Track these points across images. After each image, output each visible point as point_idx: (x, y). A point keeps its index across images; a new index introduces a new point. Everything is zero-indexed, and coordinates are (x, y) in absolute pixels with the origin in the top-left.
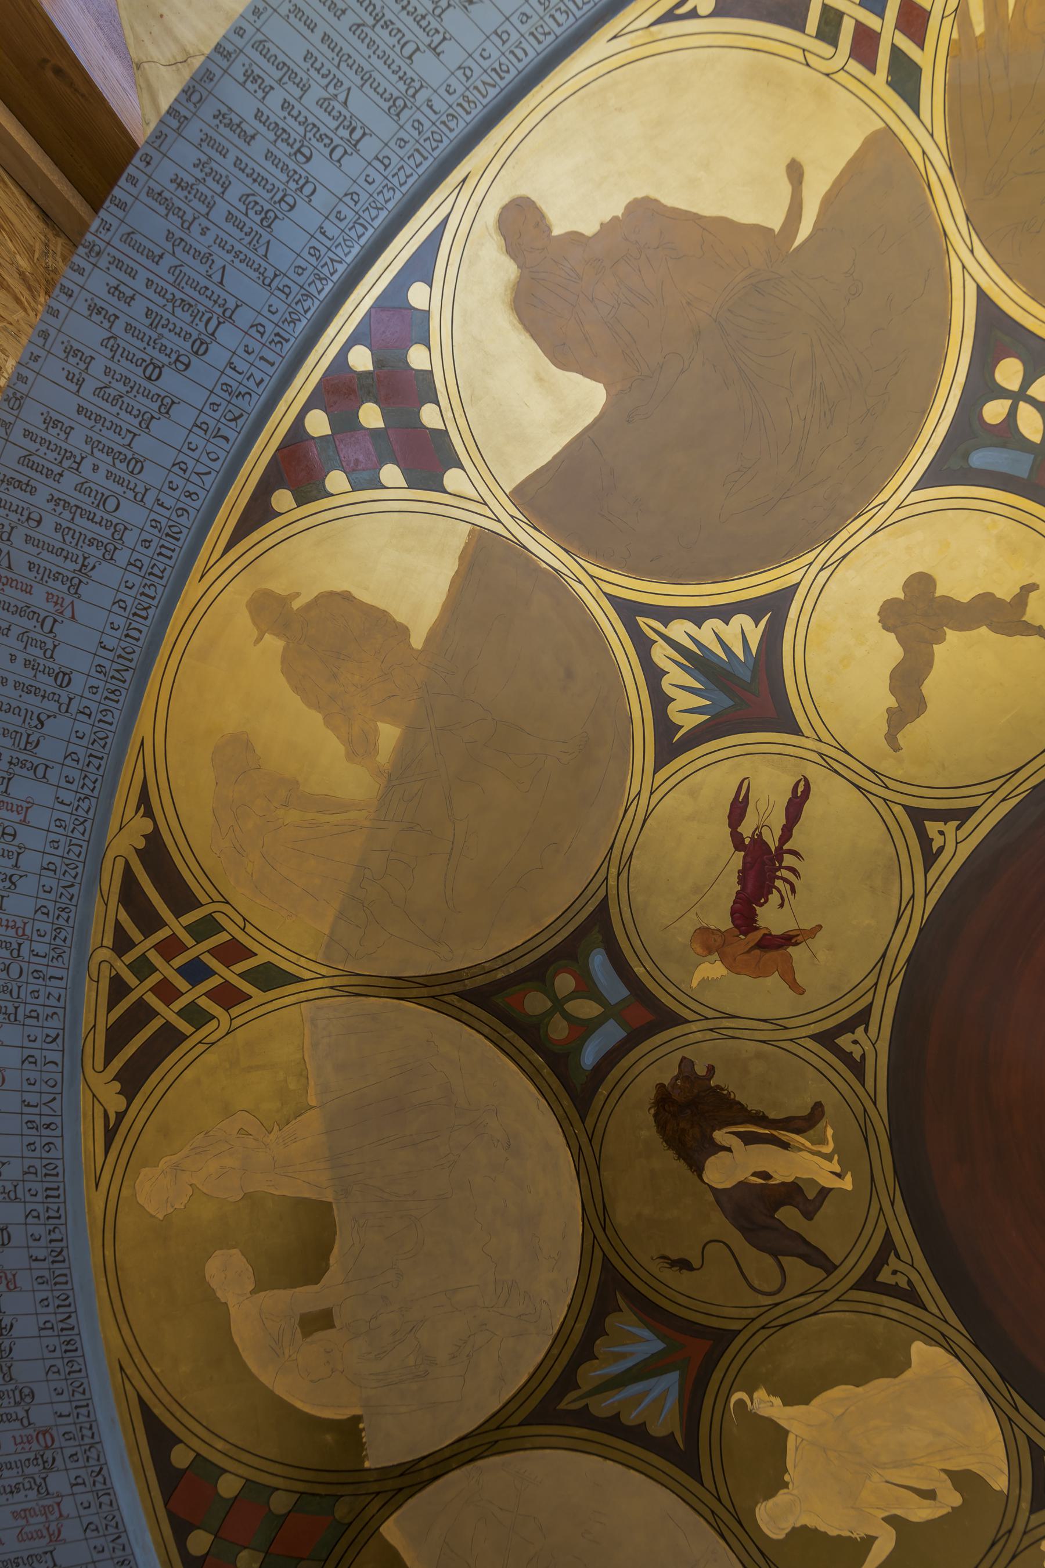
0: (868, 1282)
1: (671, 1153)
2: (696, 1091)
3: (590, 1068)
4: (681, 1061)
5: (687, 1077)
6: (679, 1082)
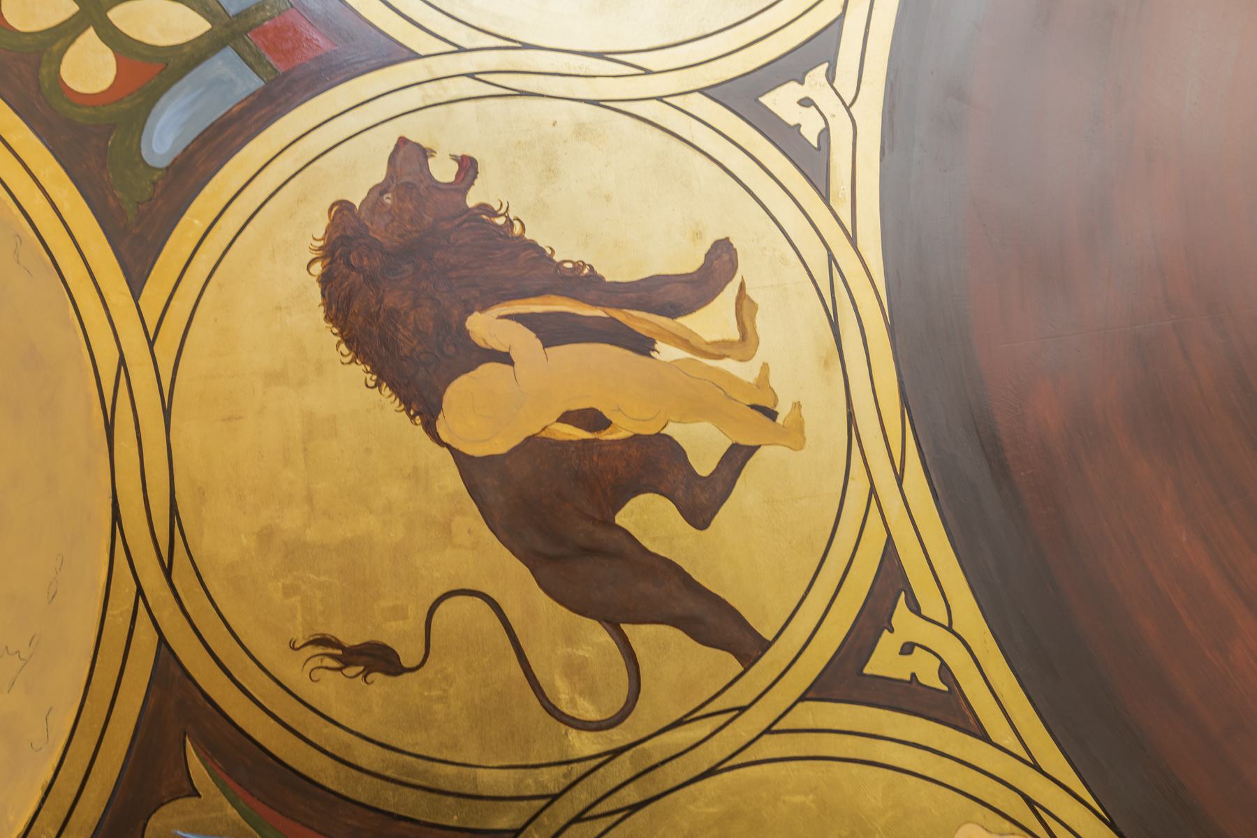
0: (845, 679)
1: (359, 372)
2: (428, 219)
3: (164, 163)
4: (397, 148)
5: (409, 187)
6: (388, 199)
